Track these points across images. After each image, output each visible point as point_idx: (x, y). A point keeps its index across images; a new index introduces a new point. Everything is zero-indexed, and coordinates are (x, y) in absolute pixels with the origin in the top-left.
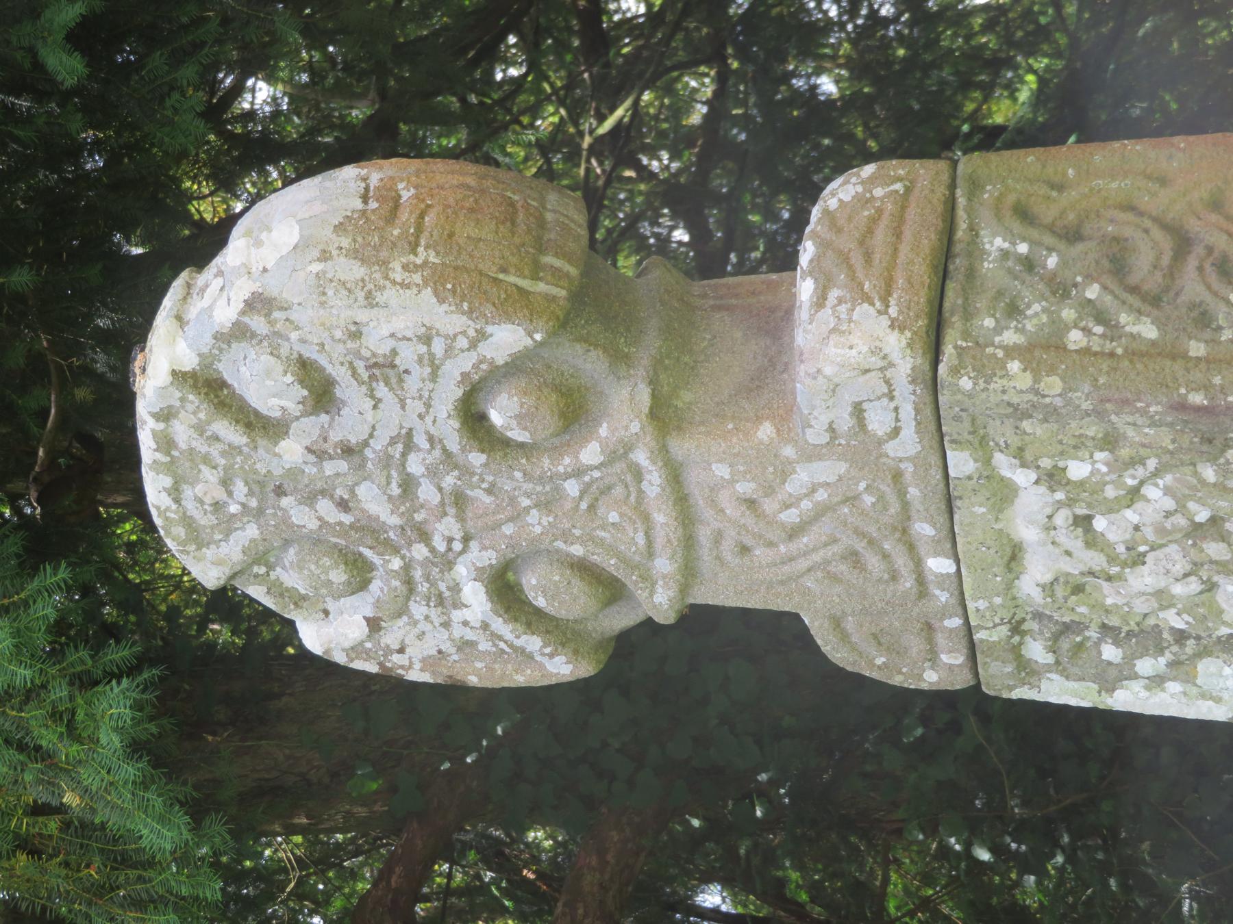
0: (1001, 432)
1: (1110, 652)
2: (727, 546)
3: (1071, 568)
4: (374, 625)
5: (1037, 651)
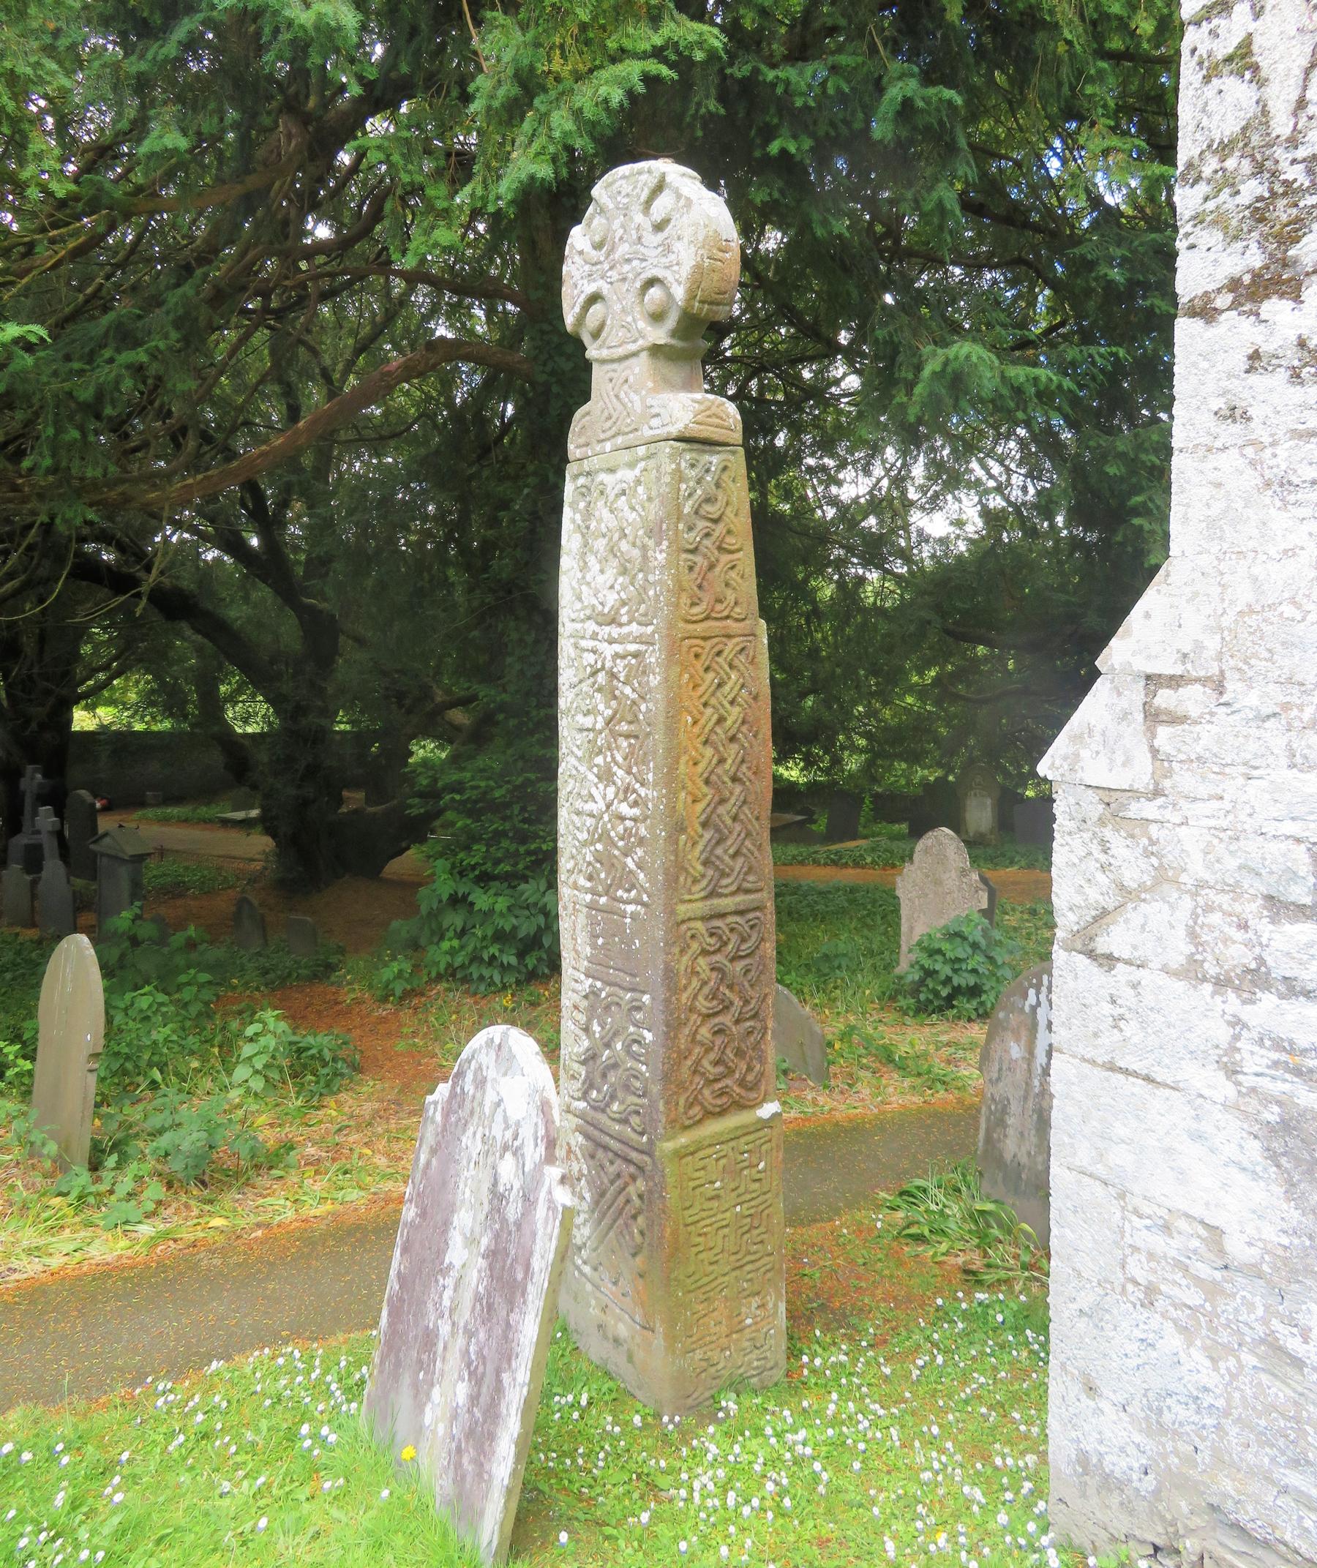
0: (652, 463)
1: (582, 505)
2: (611, 374)
3: (608, 490)
4: (581, 253)
5: (581, 481)
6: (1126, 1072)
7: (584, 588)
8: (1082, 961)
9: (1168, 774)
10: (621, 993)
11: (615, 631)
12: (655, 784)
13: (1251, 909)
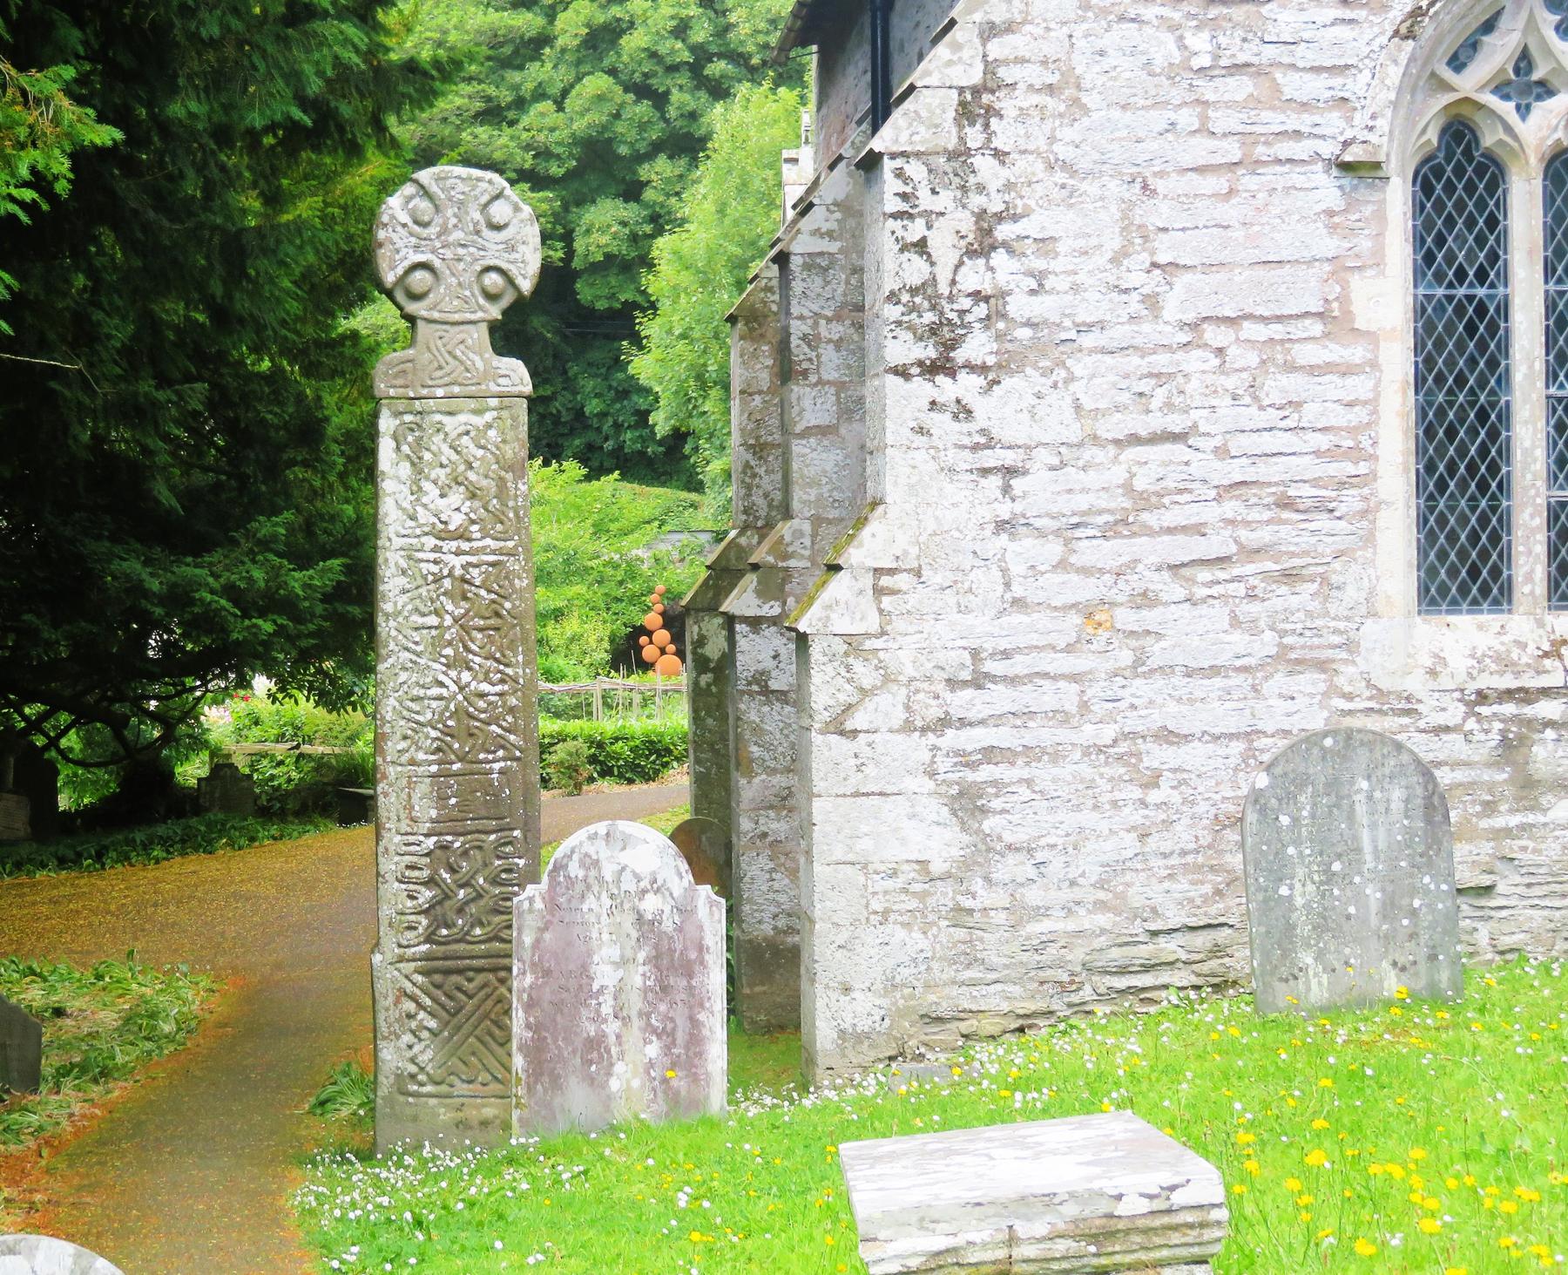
0: (505, 414)
4: (404, 225)
6: (868, 794)
7: (419, 509)
8: (834, 738)
9: (889, 623)
10: (483, 837)
11: (465, 546)
12: (526, 664)
13: (940, 687)
